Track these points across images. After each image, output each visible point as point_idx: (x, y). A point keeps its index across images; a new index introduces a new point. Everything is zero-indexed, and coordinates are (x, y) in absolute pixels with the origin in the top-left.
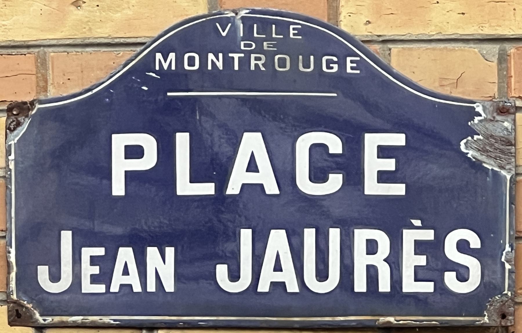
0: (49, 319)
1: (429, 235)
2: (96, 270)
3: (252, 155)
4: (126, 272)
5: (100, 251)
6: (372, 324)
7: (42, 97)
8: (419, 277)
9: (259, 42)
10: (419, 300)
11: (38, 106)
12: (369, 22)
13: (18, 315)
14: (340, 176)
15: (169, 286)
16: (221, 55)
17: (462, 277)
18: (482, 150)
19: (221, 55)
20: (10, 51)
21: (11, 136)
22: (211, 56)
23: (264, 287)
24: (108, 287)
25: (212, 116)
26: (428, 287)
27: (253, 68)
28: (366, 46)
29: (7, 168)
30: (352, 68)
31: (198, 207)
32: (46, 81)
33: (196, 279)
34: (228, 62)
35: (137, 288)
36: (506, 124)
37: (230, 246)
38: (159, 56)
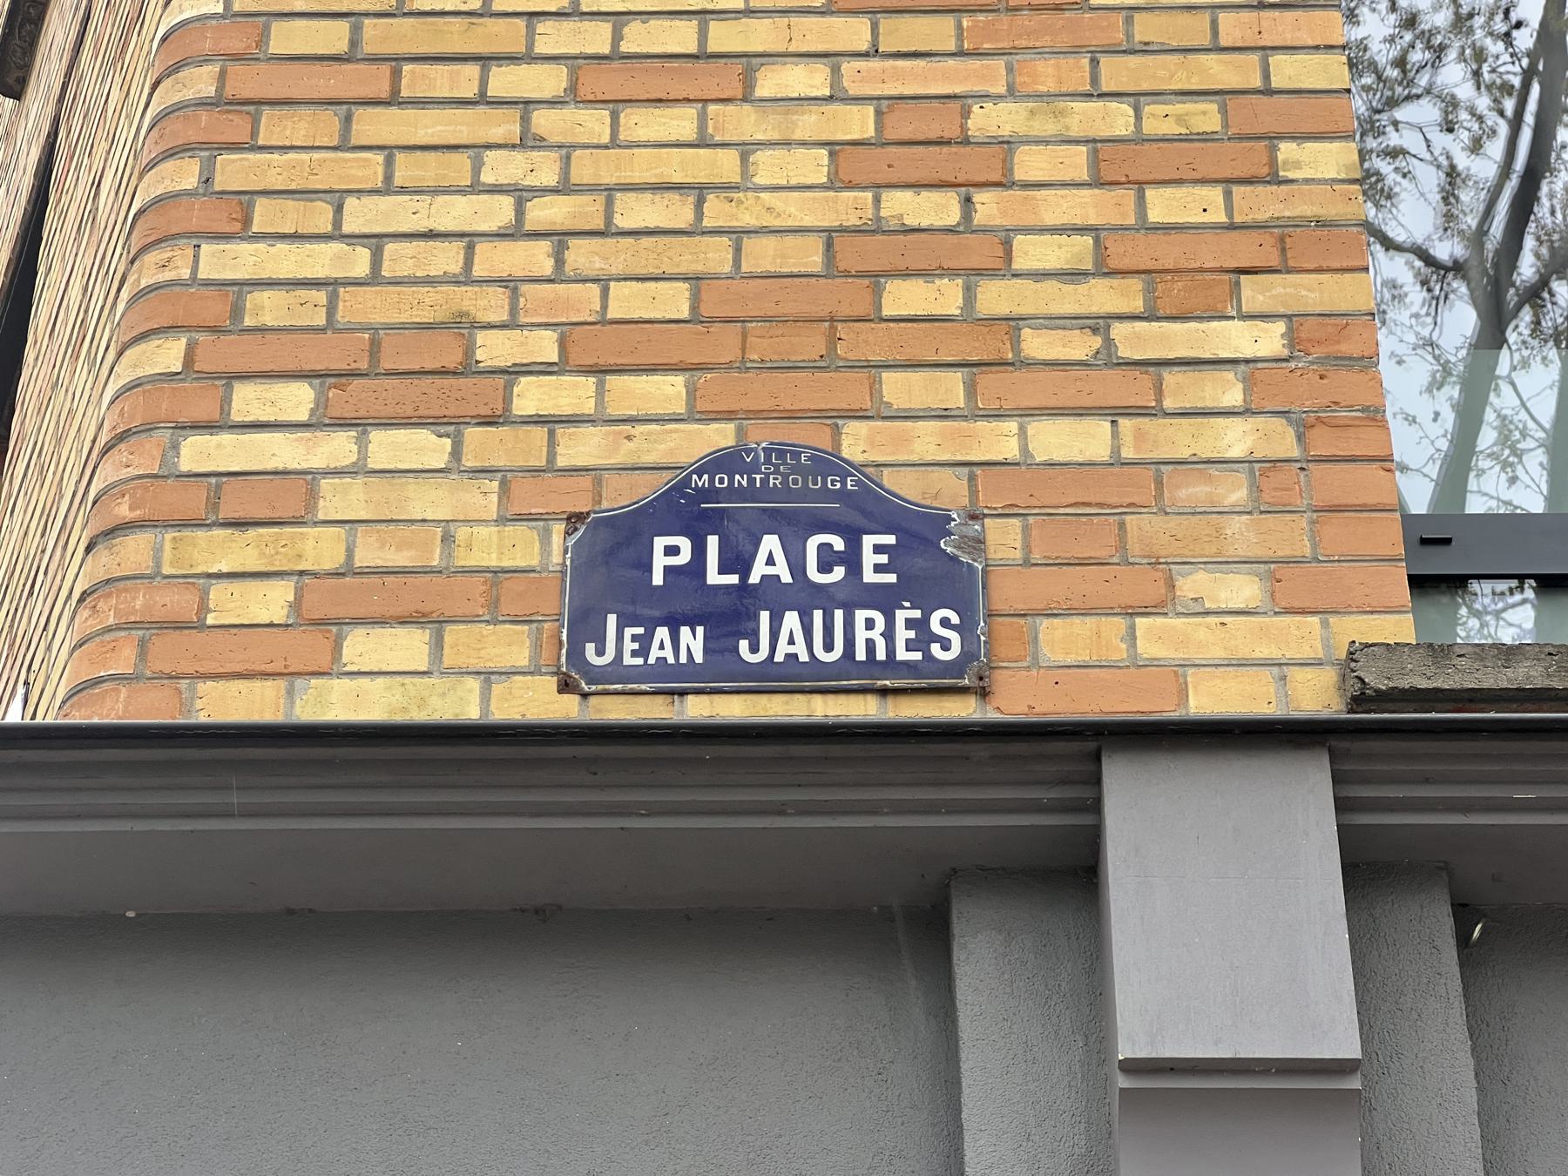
0: (594, 688)
1: (917, 614)
2: (636, 646)
3: (771, 552)
4: (662, 647)
5: (640, 630)
6: (871, 687)
7: (597, 508)
8: (910, 647)
9: (777, 466)
10: (911, 667)
11: (593, 515)
12: (865, 451)
13: (567, 684)
14: (843, 569)
15: (699, 658)
16: (745, 476)
17: (946, 646)
18: (959, 547)
19: (745, 476)
20: (572, 473)
21: (568, 539)
22: (737, 477)
23: (779, 658)
24: (646, 660)
25: (737, 522)
26: (917, 656)
27: (771, 485)
28: (863, 469)
29: (564, 564)
30: (878, 568)
31: (724, 594)
32: (601, 496)
33: (721, 652)
34: (751, 481)
35: (671, 660)
36: (976, 527)
37: (751, 625)
38: (695, 477)
